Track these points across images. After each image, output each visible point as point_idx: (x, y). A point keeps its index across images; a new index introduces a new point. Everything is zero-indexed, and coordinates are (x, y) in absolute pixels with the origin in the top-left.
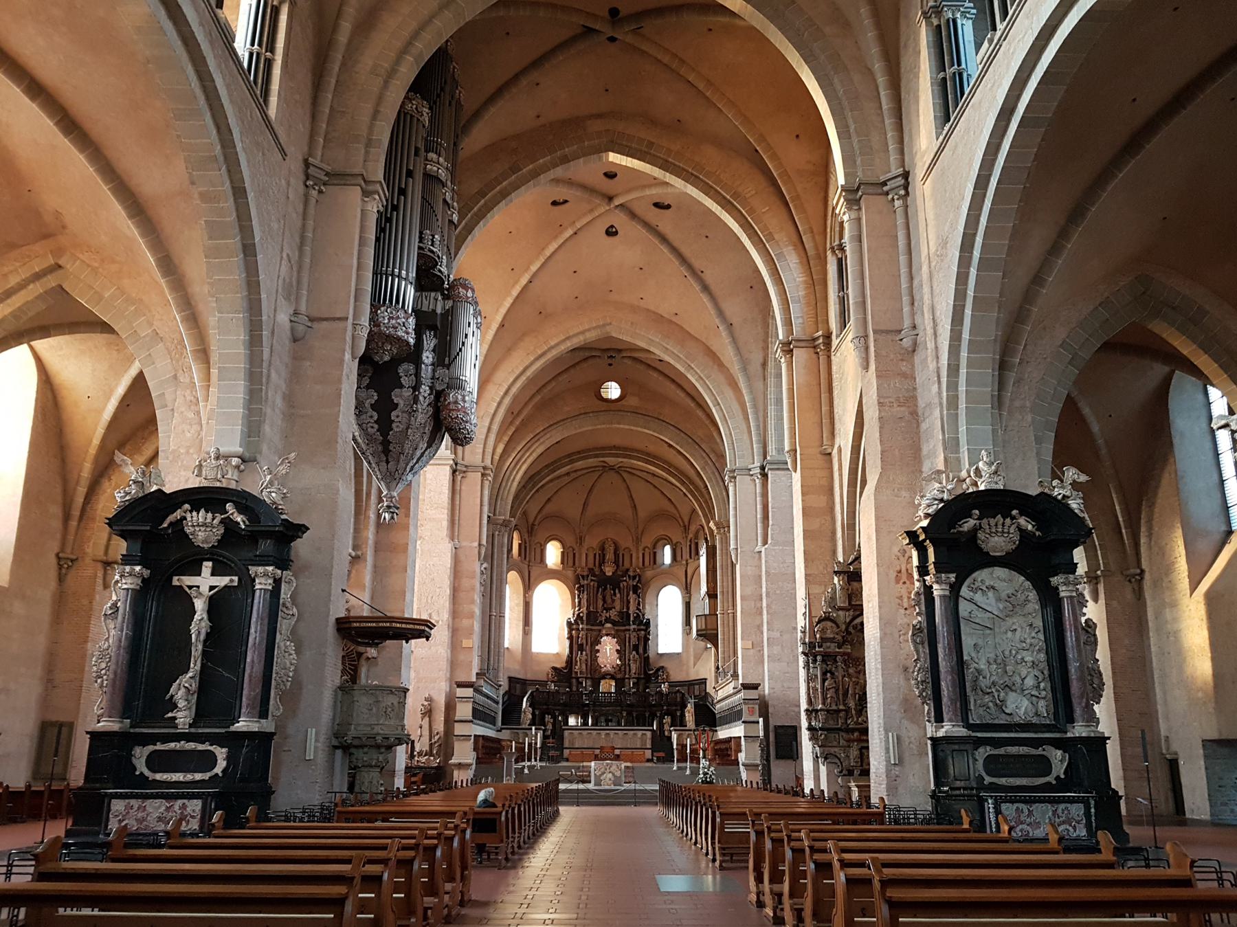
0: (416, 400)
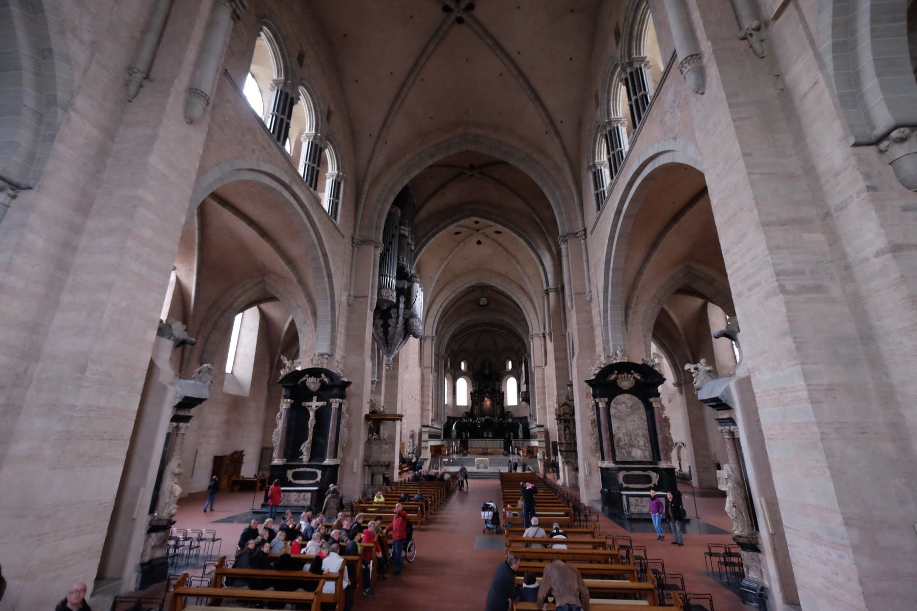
0: (397, 323)
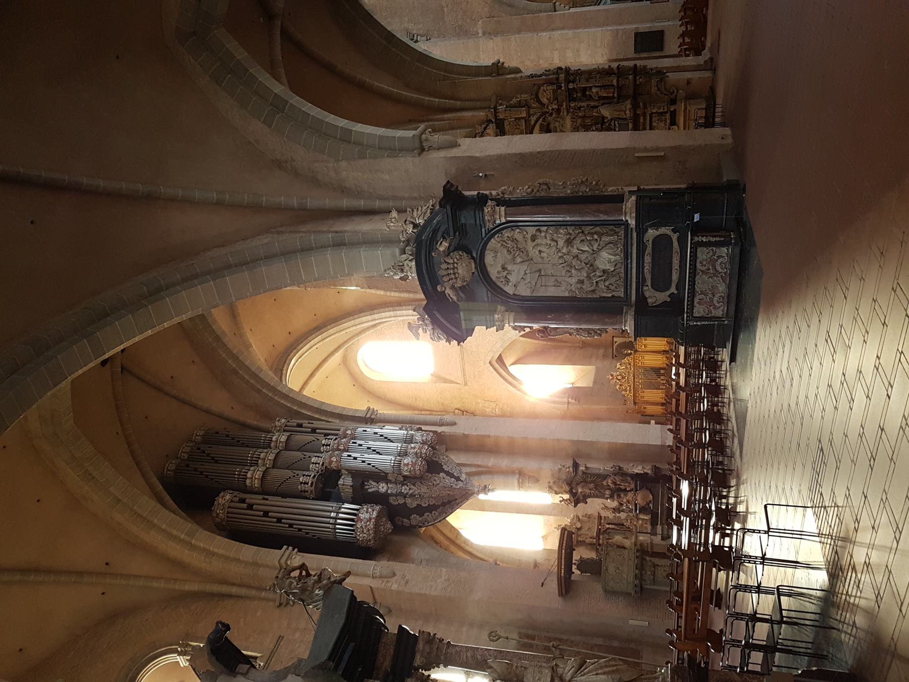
0: (412, 496)
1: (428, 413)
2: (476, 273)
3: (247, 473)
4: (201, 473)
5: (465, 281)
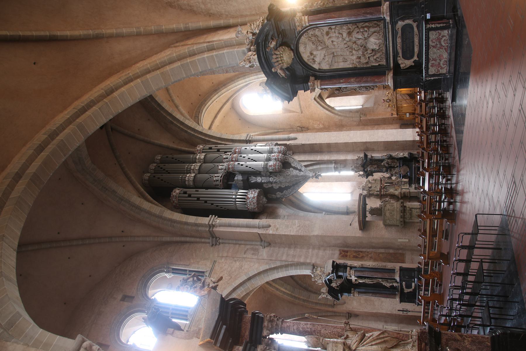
0: (276, 182)
1: (282, 130)
2: (295, 59)
3: (185, 178)
4: (162, 180)
5: (288, 64)
